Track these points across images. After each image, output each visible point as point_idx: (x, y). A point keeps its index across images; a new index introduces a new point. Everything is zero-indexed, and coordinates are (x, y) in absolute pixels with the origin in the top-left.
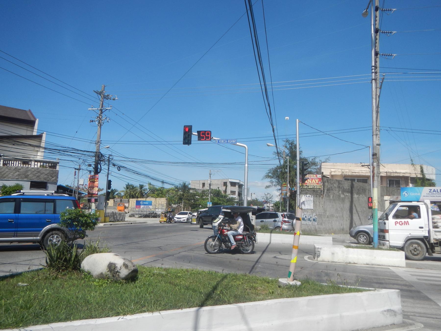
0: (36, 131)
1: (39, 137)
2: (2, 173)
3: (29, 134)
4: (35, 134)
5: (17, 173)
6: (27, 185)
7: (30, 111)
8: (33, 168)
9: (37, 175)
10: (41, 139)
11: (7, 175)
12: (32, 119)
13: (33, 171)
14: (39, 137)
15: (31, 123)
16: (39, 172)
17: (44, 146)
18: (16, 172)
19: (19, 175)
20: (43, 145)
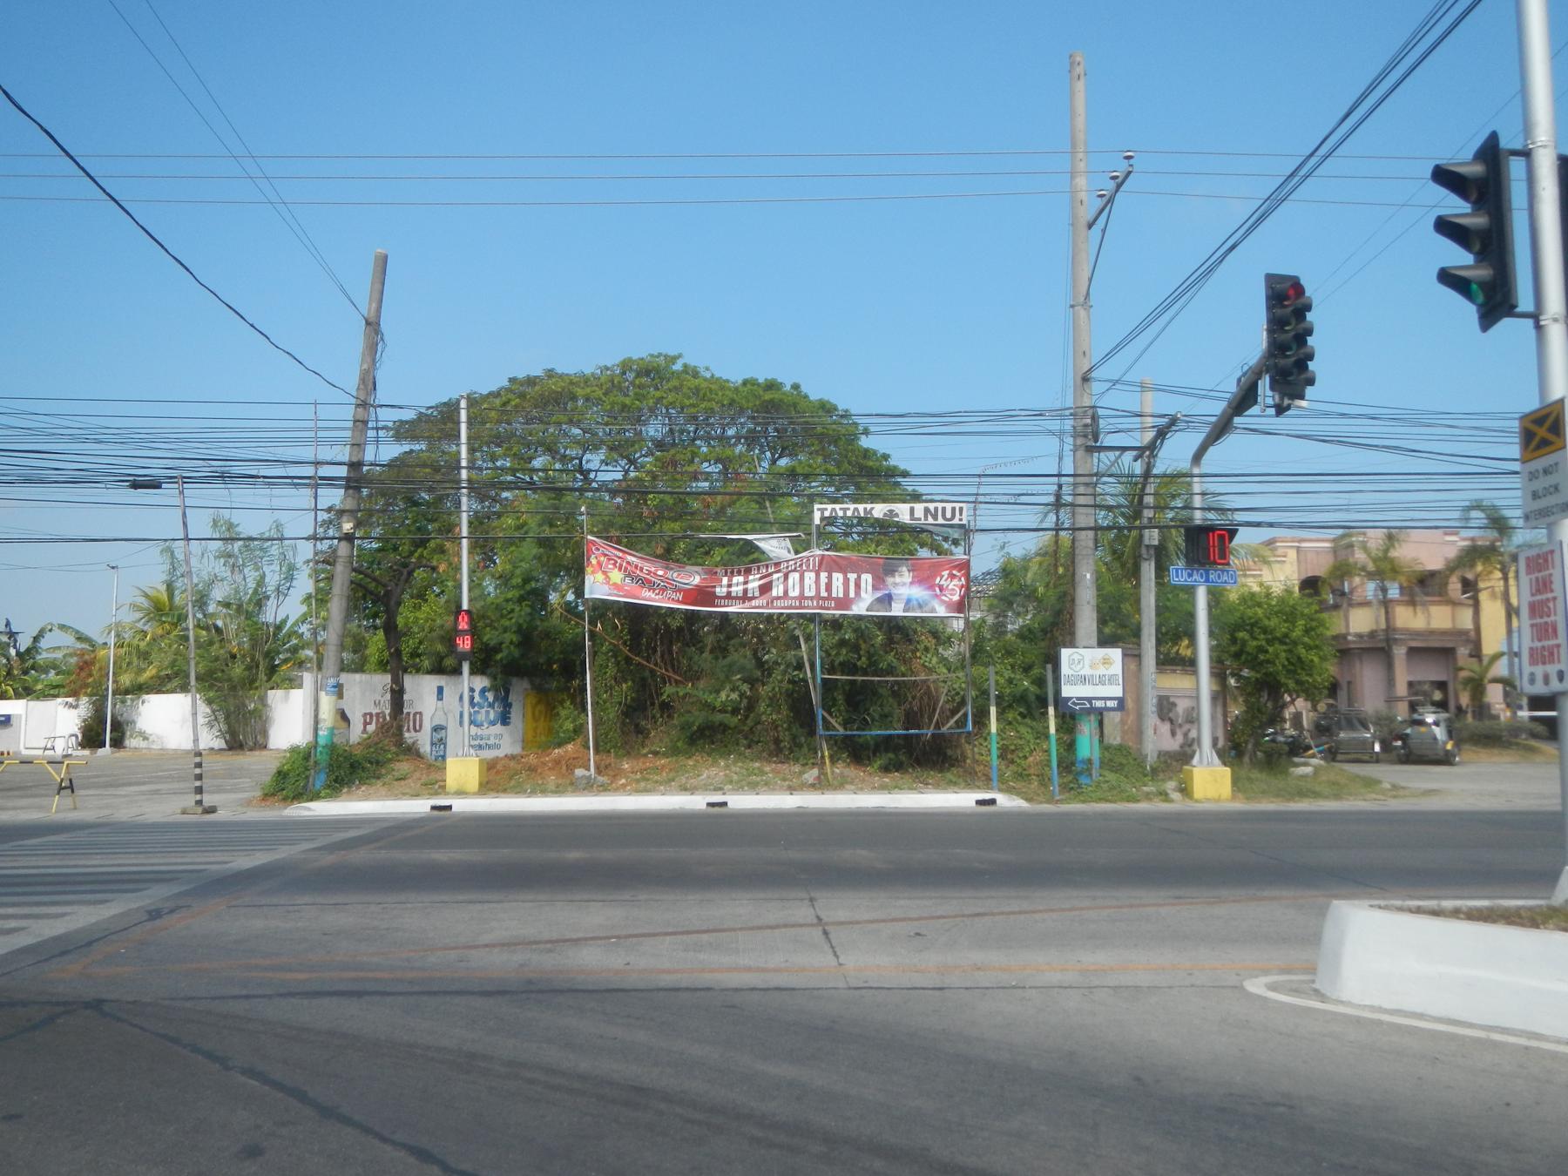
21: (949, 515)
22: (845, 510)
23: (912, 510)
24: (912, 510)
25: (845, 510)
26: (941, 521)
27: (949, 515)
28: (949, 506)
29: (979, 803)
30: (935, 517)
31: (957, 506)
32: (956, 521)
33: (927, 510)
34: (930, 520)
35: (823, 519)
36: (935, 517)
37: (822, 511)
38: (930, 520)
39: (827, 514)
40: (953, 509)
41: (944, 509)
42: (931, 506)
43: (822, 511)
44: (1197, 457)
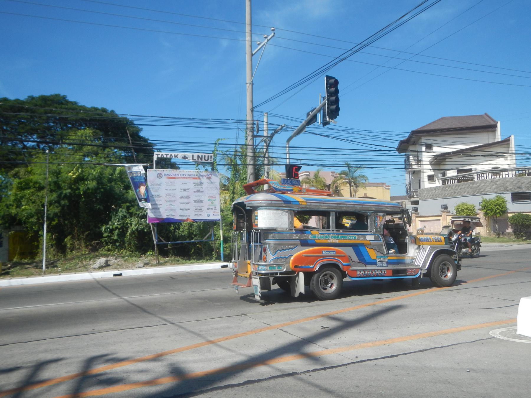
0: (499, 137)
1: (506, 142)
2: (479, 188)
3: (491, 141)
4: (499, 139)
5: (495, 186)
6: (508, 197)
7: (486, 114)
8: (511, 178)
9: (517, 185)
10: (509, 144)
11: (484, 190)
12: (493, 123)
13: (513, 182)
14: (506, 142)
15: (492, 128)
16: (519, 182)
17: (514, 152)
18: (493, 185)
19: (497, 188)
20: (513, 150)
21: (206, 158)
23: (193, 156)
24: (193, 156)
25: (167, 155)
26: (203, 161)
27: (206, 158)
29: (222, 267)
30: (202, 160)
32: (209, 161)
33: (198, 156)
34: (200, 160)
35: (158, 158)
36: (202, 160)
37: (158, 155)
38: (200, 160)
39: (160, 156)
40: (208, 156)
41: (205, 156)
43: (158, 155)
44: (289, 140)
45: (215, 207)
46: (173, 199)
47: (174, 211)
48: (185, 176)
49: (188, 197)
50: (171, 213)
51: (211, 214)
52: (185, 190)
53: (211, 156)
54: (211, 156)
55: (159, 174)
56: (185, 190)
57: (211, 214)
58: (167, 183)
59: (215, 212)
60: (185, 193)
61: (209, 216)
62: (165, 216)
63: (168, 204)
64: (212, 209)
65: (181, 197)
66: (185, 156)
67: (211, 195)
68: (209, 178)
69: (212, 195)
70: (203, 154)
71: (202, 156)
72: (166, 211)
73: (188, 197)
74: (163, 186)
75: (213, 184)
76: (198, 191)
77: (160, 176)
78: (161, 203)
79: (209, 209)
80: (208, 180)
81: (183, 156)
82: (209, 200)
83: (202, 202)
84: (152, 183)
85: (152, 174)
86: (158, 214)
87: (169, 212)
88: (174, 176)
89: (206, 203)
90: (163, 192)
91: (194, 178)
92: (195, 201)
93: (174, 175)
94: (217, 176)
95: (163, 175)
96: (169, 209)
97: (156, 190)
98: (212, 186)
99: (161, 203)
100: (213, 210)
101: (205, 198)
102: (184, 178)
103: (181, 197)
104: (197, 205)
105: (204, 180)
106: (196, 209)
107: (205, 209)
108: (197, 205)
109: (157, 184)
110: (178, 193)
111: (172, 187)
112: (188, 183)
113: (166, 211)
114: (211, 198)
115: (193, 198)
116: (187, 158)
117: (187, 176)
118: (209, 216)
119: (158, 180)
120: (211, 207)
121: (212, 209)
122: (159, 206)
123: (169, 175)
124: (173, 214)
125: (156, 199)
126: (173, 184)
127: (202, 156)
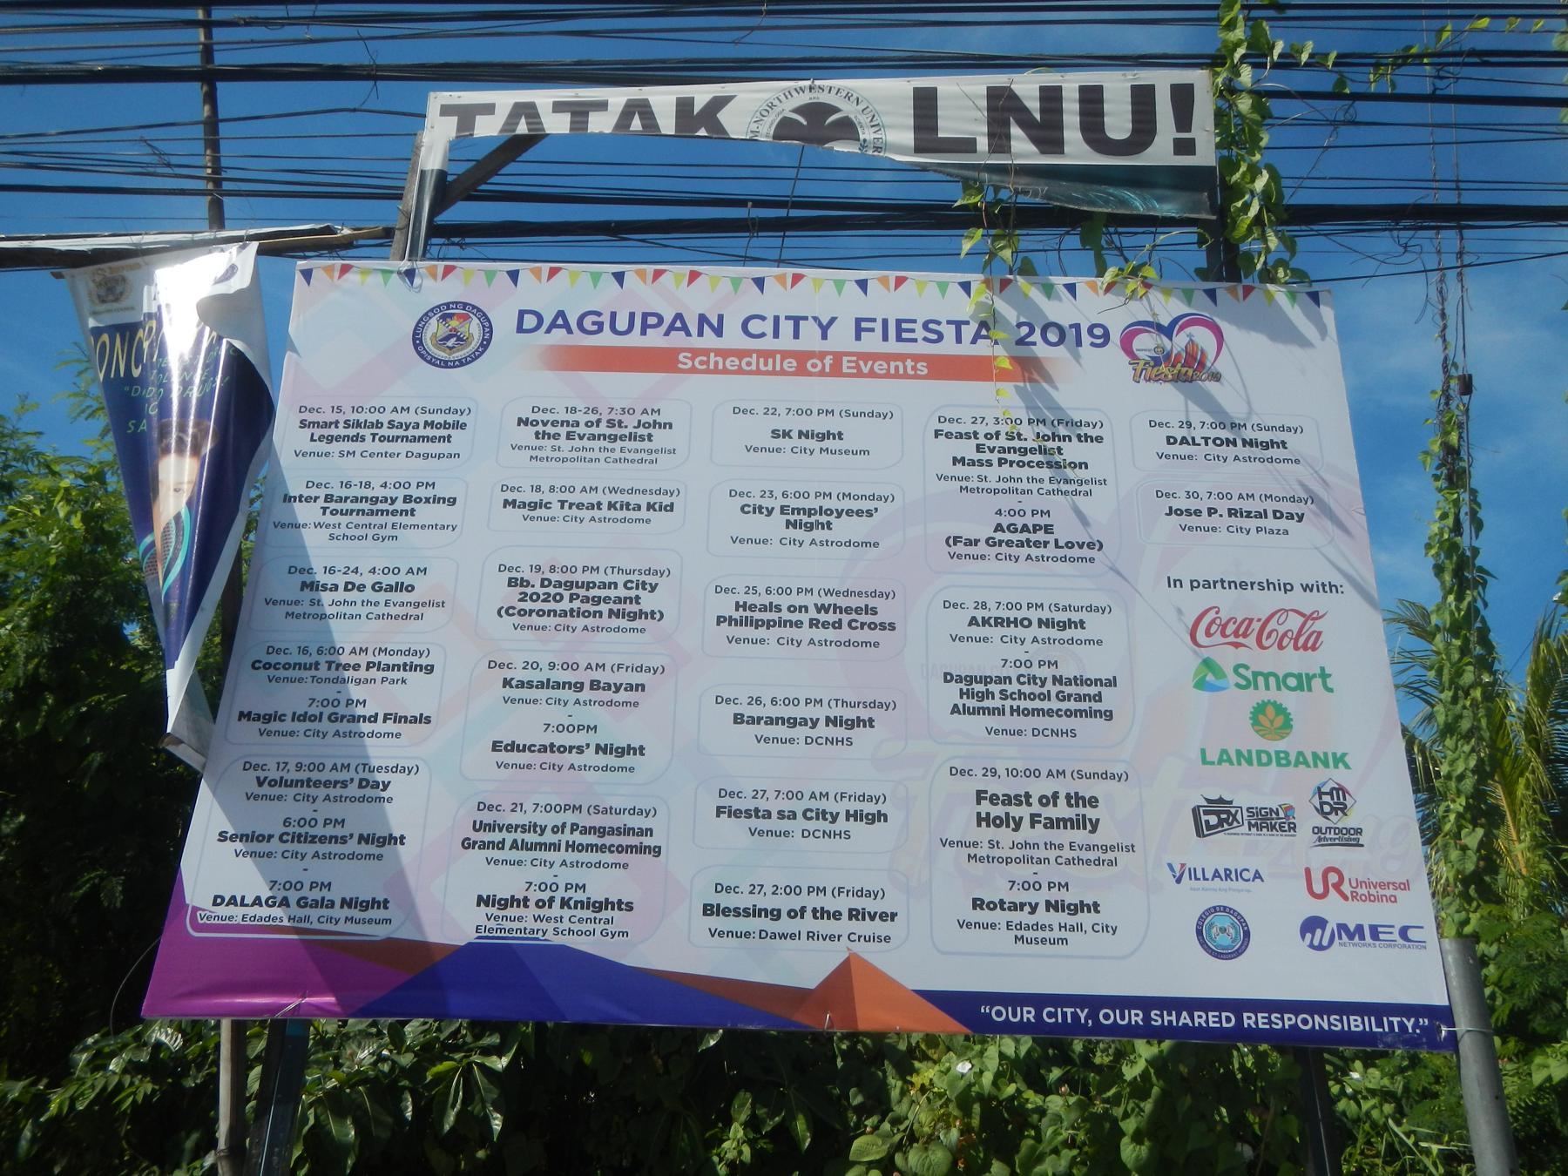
21: (1118, 124)
22: (580, 112)
23: (925, 104)
24: (925, 104)
25: (580, 112)
26: (1077, 151)
27: (1118, 124)
28: (1117, 86)
30: (1047, 133)
31: (1162, 80)
32: (1160, 153)
33: (1002, 107)
34: (1023, 150)
36: (1047, 133)
37: (466, 116)
38: (1023, 150)
40: (1143, 98)
41: (1092, 99)
42: (1027, 86)
45: (1334, 801)
46: (611, 647)
47: (626, 839)
48: (810, 338)
49: (853, 617)
50: (560, 871)
51: (1274, 908)
52: (806, 519)
53: (1183, 98)
54: (1183, 98)
55: (444, 312)
56: (806, 519)
57: (1274, 908)
58: (540, 426)
59: (1332, 882)
60: (815, 568)
61: (1223, 935)
62: (449, 904)
63: (528, 723)
64: (1268, 821)
65: (752, 617)
66: (817, 112)
67: (1229, 604)
68: (1189, 370)
69: (1261, 604)
70: (1071, 83)
71: (1051, 97)
72: (487, 834)
73: (853, 617)
74: (486, 464)
75: (1233, 435)
76: (1024, 535)
77: (451, 339)
78: (413, 694)
79: (1215, 817)
80: (1167, 400)
81: (787, 108)
82: (1208, 676)
83: (1086, 699)
84: (337, 430)
85: (349, 329)
86: (351, 879)
87: (529, 841)
88: (655, 339)
89: (1162, 741)
90: (467, 555)
91: (944, 368)
92: (975, 694)
93: (649, 321)
94: (1284, 333)
95: (504, 322)
96: (536, 794)
97: (377, 510)
98: (1241, 476)
99: (413, 694)
100: (1301, 850)
101: (1141, 647)
102: (802, 363)
103: (752, 617)
104: (1009, 754)
105: (1094, 384)
106: (997, 811)
107: (1148, 808)
108: (1009, 754)
109: (401, 432)
110: (700, 552)
111: (605, 473)
112: (856, 433)
113: (487, 834)
114: (1243, 641)
115: (929, 644)
116: (847, 129)
117: (842, 337)
118: (1223, 935)
119: (421, 388)
120: (1251, 789)
121: (1268, 821)
122: (379, 752)
123: (591, 322)
124: (601, 884)
125: (346, 635)
126: (633, 432)
127: (1051, 97)
